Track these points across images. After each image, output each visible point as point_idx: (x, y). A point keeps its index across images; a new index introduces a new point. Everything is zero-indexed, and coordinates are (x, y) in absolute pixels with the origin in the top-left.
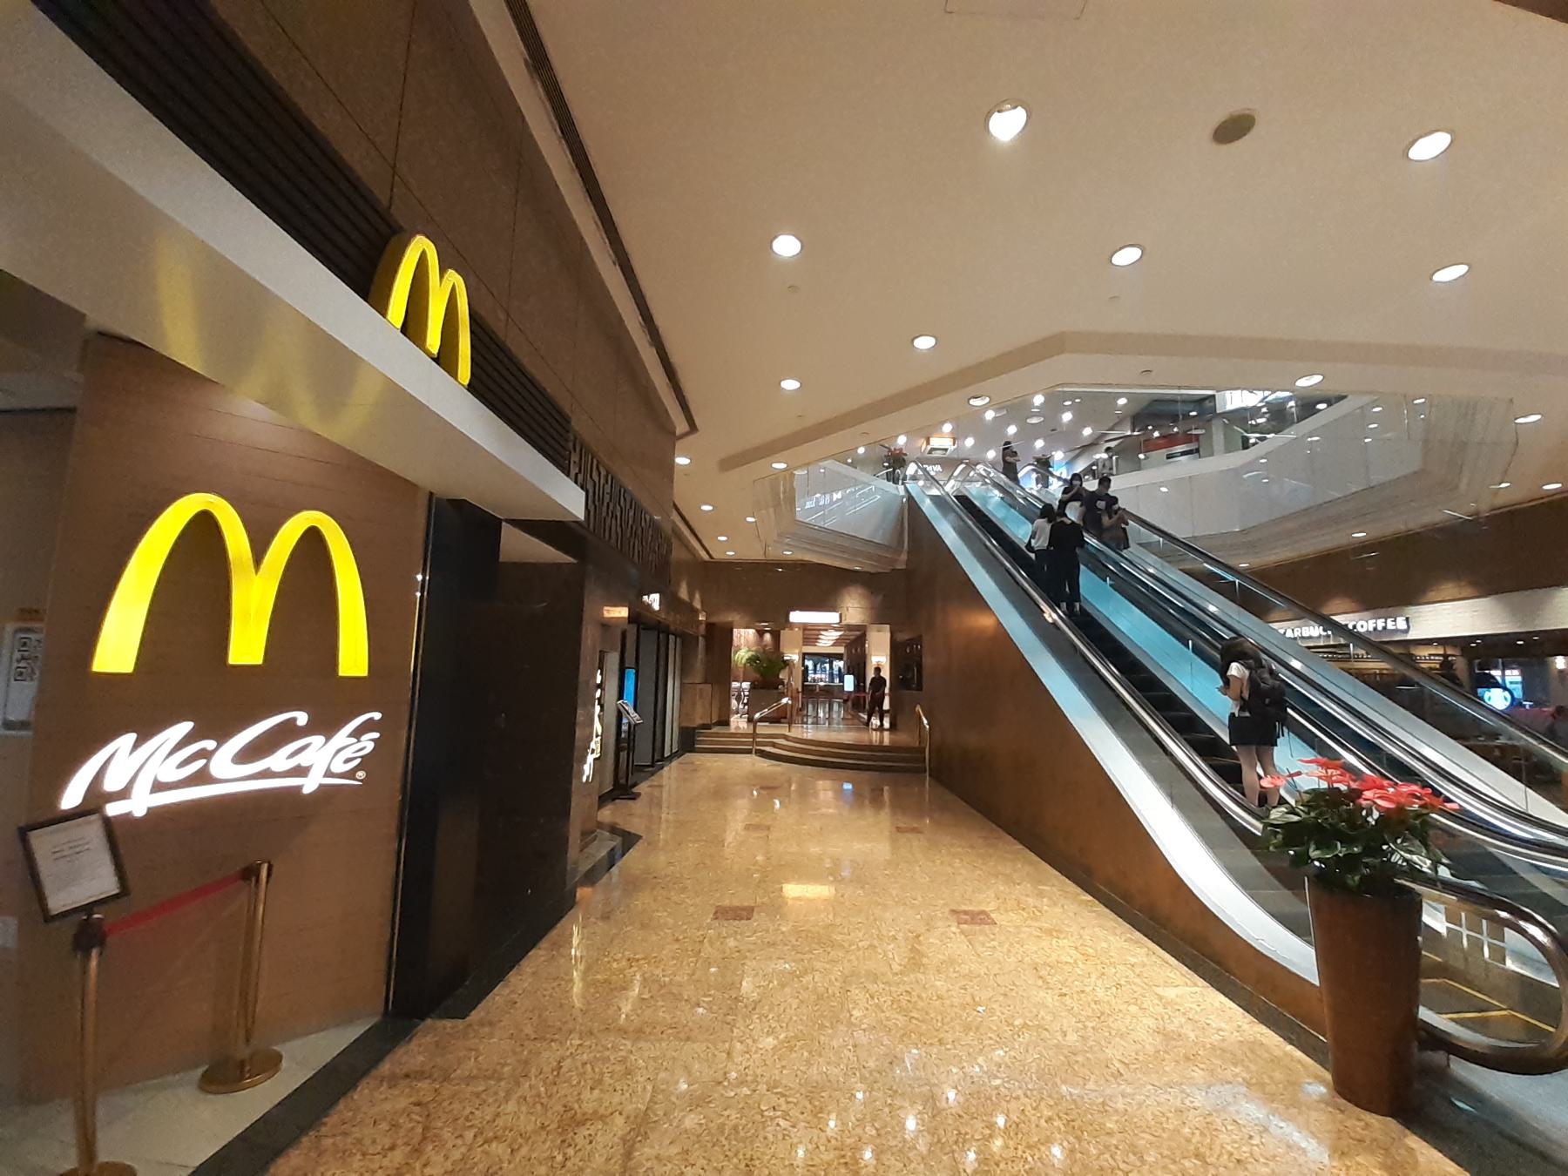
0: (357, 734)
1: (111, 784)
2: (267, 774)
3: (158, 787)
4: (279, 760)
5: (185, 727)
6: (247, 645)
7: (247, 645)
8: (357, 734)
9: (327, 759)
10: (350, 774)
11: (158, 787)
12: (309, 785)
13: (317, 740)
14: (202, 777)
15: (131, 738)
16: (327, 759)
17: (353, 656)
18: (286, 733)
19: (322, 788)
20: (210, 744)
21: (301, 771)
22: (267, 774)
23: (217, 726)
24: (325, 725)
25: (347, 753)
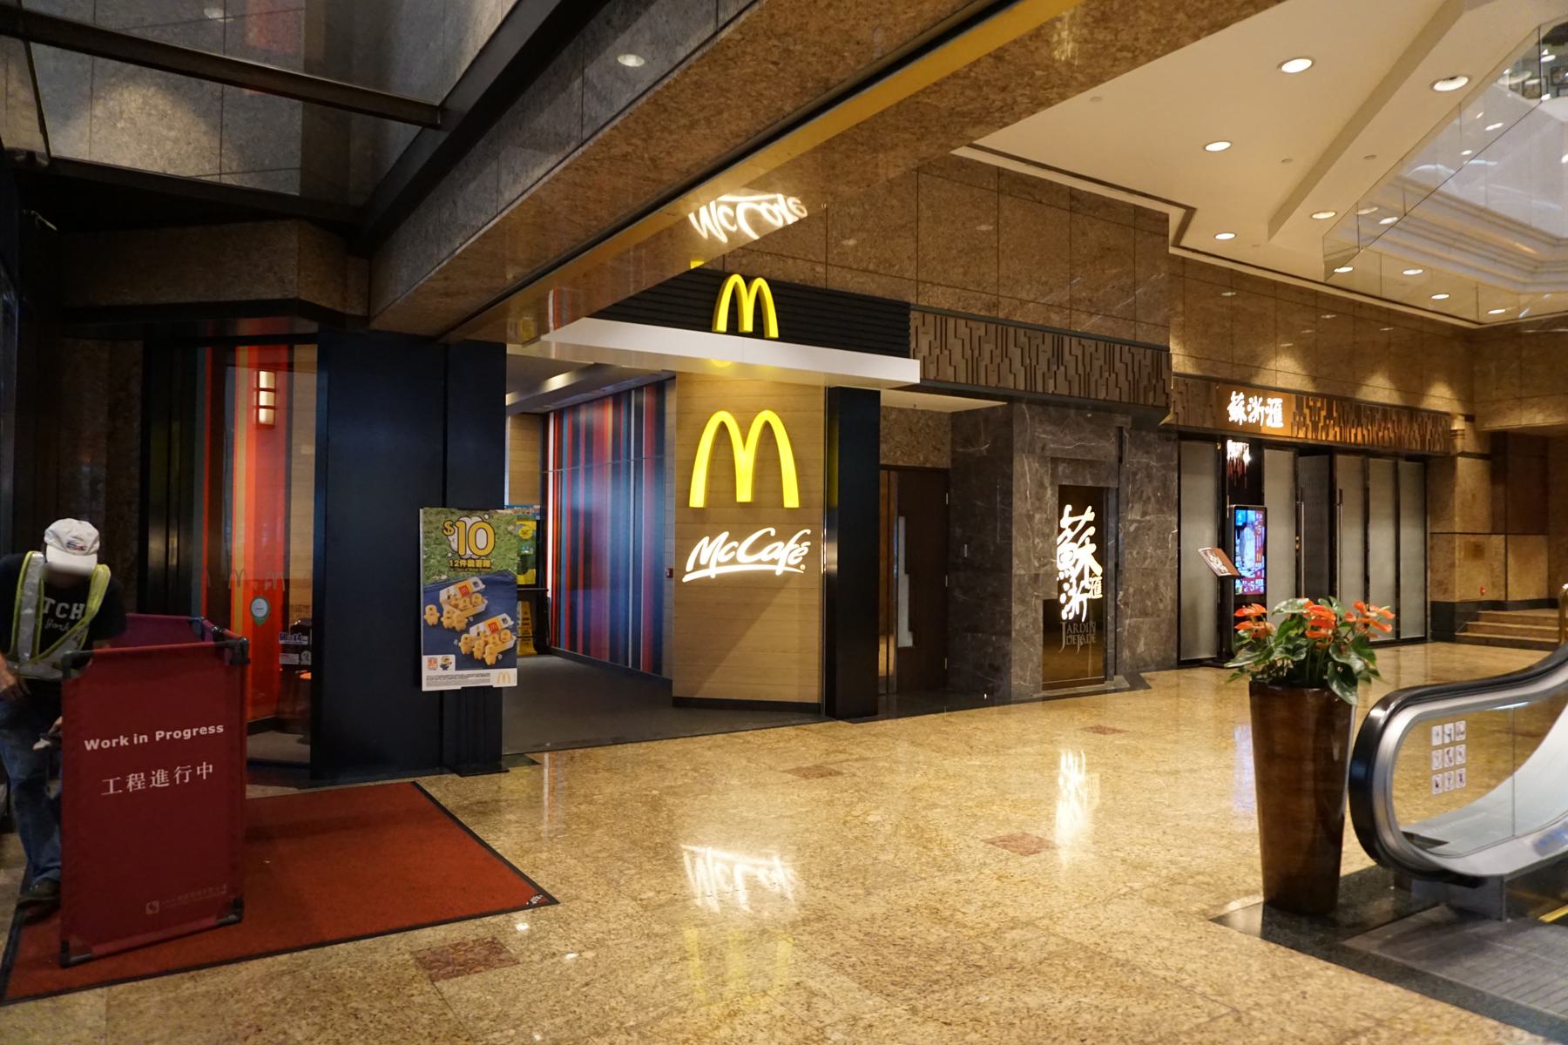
0: (799, 542)
1: (703, 562)
2: (759, 562)
3: (719, 564)
4: (764, 555)
5: (725, 535)
6: (744, 493)
7: (744, 493)
8: (799, 542)
9: (784, 555)
10: (797, 566)
11: (719, 564)
12: (779, 570)
13: (780, 544)
14: (733, 561)
15: (707, 539)
16: (784, 555)
17: (791, 499)
18: (765, 540)
19: (785, 572)
20: (735, 544)
21: (774, 562)
22: (759, 562)
23: (738, 536)
24: (784, 536)
25: (795, 553)
